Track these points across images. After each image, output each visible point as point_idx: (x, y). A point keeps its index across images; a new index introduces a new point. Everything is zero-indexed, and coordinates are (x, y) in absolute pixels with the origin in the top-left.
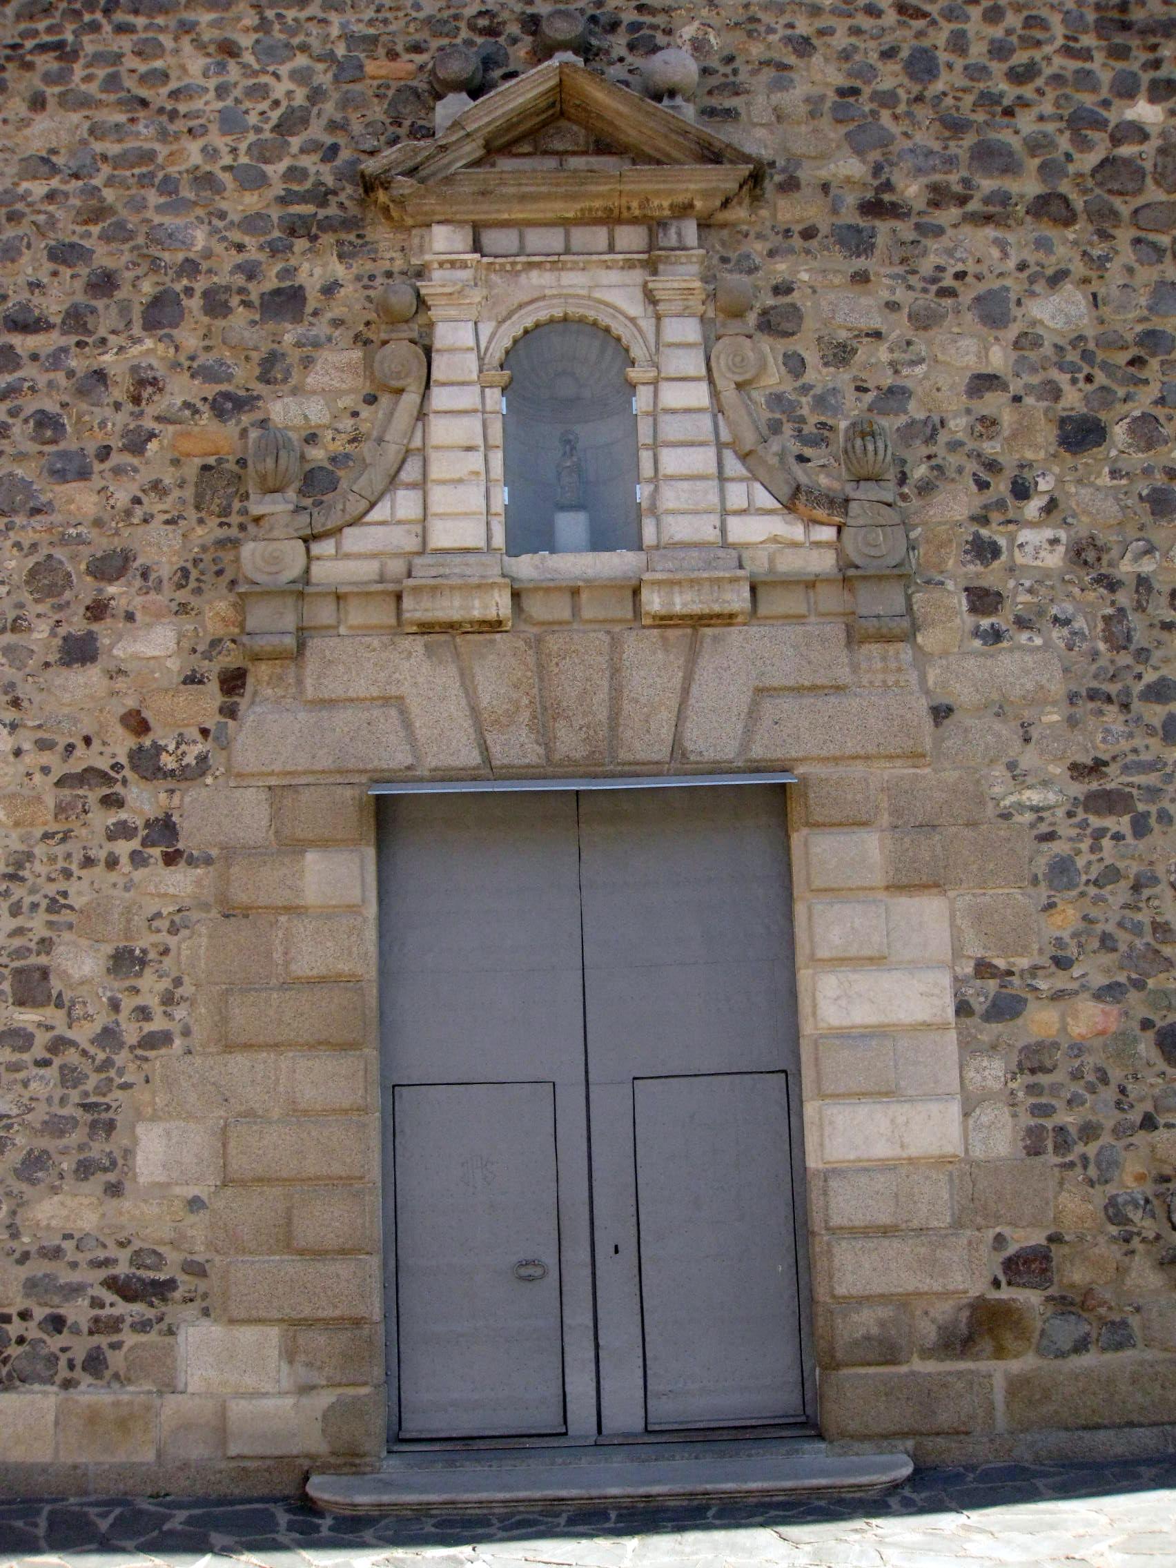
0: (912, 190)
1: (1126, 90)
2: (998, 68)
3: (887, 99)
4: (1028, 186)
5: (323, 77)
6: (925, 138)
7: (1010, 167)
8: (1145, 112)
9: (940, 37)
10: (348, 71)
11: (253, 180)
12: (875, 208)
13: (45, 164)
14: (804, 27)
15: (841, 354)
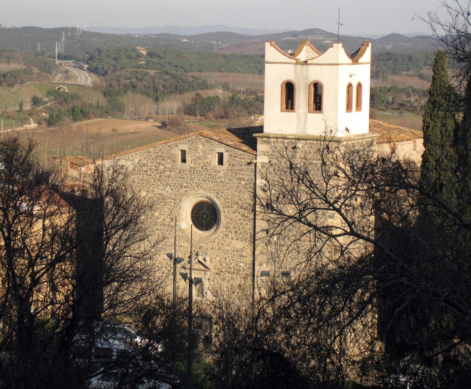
1: (241, 262)
2: (231, 259)
3: (223, 262)
5: (183, 254)
6: (225, 265)
8: (242, 265)
9: (227, 256)
10: (185, 254)
14: (217, 254)
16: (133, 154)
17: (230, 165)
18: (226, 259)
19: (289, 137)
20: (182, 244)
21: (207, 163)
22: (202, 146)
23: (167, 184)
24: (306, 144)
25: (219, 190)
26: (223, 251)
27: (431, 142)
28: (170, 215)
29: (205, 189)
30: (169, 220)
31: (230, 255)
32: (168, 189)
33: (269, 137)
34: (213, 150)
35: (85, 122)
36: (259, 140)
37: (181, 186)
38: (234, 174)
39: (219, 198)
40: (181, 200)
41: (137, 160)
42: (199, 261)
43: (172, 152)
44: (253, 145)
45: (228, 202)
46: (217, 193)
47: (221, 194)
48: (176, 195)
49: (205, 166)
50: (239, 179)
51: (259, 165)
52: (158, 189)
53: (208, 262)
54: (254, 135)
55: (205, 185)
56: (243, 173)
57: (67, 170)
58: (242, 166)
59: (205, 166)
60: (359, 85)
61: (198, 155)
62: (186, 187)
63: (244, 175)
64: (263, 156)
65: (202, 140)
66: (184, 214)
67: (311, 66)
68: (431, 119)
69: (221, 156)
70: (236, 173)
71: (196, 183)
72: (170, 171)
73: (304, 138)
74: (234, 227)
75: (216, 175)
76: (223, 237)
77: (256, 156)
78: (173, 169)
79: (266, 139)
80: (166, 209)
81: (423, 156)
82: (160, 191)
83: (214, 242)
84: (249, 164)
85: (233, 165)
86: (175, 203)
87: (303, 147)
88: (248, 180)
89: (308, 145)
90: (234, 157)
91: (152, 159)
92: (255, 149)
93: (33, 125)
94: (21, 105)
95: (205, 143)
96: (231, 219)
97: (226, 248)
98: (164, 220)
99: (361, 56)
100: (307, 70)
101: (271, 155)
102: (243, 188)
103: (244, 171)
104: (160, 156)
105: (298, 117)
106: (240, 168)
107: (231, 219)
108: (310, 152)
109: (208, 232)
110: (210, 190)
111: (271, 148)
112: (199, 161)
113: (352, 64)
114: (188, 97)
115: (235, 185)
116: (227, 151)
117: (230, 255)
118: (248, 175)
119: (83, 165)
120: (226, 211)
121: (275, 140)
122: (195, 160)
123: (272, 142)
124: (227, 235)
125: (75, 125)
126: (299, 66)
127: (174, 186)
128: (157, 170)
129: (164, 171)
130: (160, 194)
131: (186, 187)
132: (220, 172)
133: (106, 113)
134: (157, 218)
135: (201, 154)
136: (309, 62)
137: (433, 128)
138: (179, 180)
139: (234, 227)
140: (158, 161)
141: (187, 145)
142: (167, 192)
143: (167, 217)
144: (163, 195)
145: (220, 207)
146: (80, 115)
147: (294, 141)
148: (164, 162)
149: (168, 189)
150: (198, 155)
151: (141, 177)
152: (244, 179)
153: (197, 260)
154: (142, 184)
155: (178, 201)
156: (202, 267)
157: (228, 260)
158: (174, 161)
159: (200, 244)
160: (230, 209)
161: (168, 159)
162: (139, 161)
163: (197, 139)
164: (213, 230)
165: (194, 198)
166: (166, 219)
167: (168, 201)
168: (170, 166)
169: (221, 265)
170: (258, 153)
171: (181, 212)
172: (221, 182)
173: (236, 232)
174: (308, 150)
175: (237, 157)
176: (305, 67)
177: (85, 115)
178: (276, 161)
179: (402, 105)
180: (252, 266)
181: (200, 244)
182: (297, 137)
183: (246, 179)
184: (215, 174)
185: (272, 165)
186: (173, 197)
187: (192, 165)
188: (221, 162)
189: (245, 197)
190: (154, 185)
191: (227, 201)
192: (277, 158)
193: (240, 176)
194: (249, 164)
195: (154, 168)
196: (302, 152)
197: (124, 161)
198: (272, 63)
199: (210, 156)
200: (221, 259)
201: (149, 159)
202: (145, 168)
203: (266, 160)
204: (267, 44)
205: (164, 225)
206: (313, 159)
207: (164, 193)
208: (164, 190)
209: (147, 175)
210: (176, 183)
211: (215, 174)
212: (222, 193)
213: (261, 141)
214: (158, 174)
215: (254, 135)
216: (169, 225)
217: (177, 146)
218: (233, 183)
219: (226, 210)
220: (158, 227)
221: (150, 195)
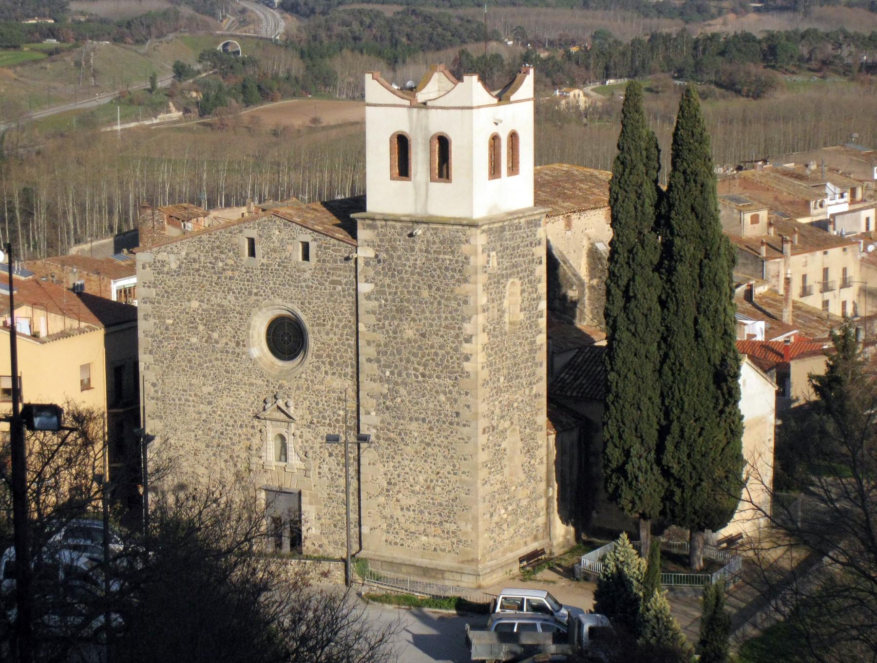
0: (315, 421)
1: (339, 409)
4: (327, 422)
6: (317, 414)
7: (325, 419)
10: (258, 397)
11: (249, 410)
12: (311, 423)
13: (228, 404)
15: (307, 442)
16: (178, 244)
17: (319, 261)
18: (317, 404)
19: (402, 218)
20: (253, 381)
21: (286, 258)
22: (277, 233)
23: (230, 289)
24: (428, 229)
25: (305, 299)
26: (314, 391)
27: (620, 223)
28: (234, 337)
29: (285, 298)
30: (234, 344)
31: (324, 398)
32: (231, 297)
33: (373, 219)
34: (294, 239)
36: (359, 223)
37: (250, 293)
38: (325, 275)
39: (305, 311)
40: (249, 314)
41: (183, 253)
42: (279, 408)
43: (235, 240)
44: (351, 229)
45: (319, 318)
46: (302, 303)
47: (307, 305)
48: (242, 306)
49: (283, 262)
50: (333, 282)
51: (361, 262)
52: (216, 297)
53: (292, 409)
54: (352, 216)
55: (283, 291)
56: (338, 272)
57: (163, 228)
58: (336, 262)
59: (283, 262)
60: (513, 137)
61: (272, 245)
62: (256, 294)
63: (340, 276)
64: (366, 247)
65: (278, 222)
66: (256, 335)
67: (434, 111)
68: (621, 188)
69: (306, 247)
70: (328, 273)
71: (271, 289)
72: (232, 270)
73: (424, 220)
74: (329, 356)
75: (300, 276)
76: (312, 371)
77: (356, 247)
78: (237, 266)
79: (370, 222)
80: (228, 328)
81: (611, 244)
82: (219, 301)
83: (300, 377)
84: (347, 259)
85: (324, 261)
86: (241, 319)
87: (424, 233)
88: (346, 284)
89: (431, 231)
90: (325, 248)
91: (207, 252)
92: (355, 236)
93: (176, 114)
94: (153, 80)
95: (282, 227)
96: (323, 343)
97: (317, 387)
98: (227, 344)
99: (516, 89)
100: (427, 117)
101: (379, 246)
102: (340, 295)
103: (340, 270)
104: (218, 247)
105: (416, 188)
106: (335, 265)
107: (323, 343)
108: (434, 243)
109: (288, 362)
110: (291, 298)
111: (378, 235)
112: (274, 255)
113: (498, 105)
115: (328, 291)
116: (315, 240)
117: (324, 398)
118: (346, 277)
119: (189, 220)
120: (316, 331)
121: (384, 223)
122: (268, 253)
123: (379, 226)
124: (318, 368)
125: (246, 113)
126: (415, 110)
127: (239, 293)
128: (213, 268)
129: (224, 270)
130: (219, 305)
131: (256, 294)
132: (305, 271)
134: (217, 342)
135: (277, 244)
136: (429, 104)
137: (623, 201)
138: (246, 283)
139: (329, 356)
140: (215, 255)
141: (256, 230)
142: (230, 302)
143: (230, 340)
144: (223, 306)
145: (307, 325)
147: (411, 224)
148: (223, 256)
149: (231, 297)
150: (272, 245)
151: (190, 278)
152: (341, 284)
153: (275, 406)
154: (193, 289)
155: (245, 316)
156: (282, 416)
157: (320, 406)
158: (238, 255)
159: (280, 382)
160: (321, 328)
161: (229, 251)
162: (187, 254)
163: (271, 221)
164: (298, 359)
165: (268, 310)
166: (230, 343)
167: (231, 315)
168: (233, 263)
169: (311, 413)
170: (359, 243)
171: (250, 332)
172: (307, 287)
173: (331, 364)
174: (431, 239)
175: (329, 248)
176: (423, 111)
177: (265, 94)
178: (385, 255)
179: (825, 63)
180: (355, 415)
181: (280, 382)
182: (414, 219)
183: (344, 282)
184: (298, 274)
185: (379, 261)
186: (238, 309)
187: (265, 261)
188: (306, 257)
189: (343, 310)
190: (209, 291)
191: (317, 315)
192: (387, 251)
193: (335, 278)
194: (347, 259)
195: (209, 265)
196: (423, 241)
197: (165, 254)
198: (375, 105)
199: (290, 247)
200: (311, 404)
201: (202, 251)
202: (196, 266)
203: (370, 253)
204: (368, 77)
205: (227, 352)
206: (439, 253)
207: (225, 303)
208: (225, 299)
209: (199, 275)
210: (241, 289)
211: (298, 274)
212: (309, 303)
213: (363, 225)
214: (215, 273)
215: (352, 216)
216: (233, 353)
217: (241, 231)
218: (325, 289)
219: (316, 329)
220: (219, 356)
221: (205, 306)
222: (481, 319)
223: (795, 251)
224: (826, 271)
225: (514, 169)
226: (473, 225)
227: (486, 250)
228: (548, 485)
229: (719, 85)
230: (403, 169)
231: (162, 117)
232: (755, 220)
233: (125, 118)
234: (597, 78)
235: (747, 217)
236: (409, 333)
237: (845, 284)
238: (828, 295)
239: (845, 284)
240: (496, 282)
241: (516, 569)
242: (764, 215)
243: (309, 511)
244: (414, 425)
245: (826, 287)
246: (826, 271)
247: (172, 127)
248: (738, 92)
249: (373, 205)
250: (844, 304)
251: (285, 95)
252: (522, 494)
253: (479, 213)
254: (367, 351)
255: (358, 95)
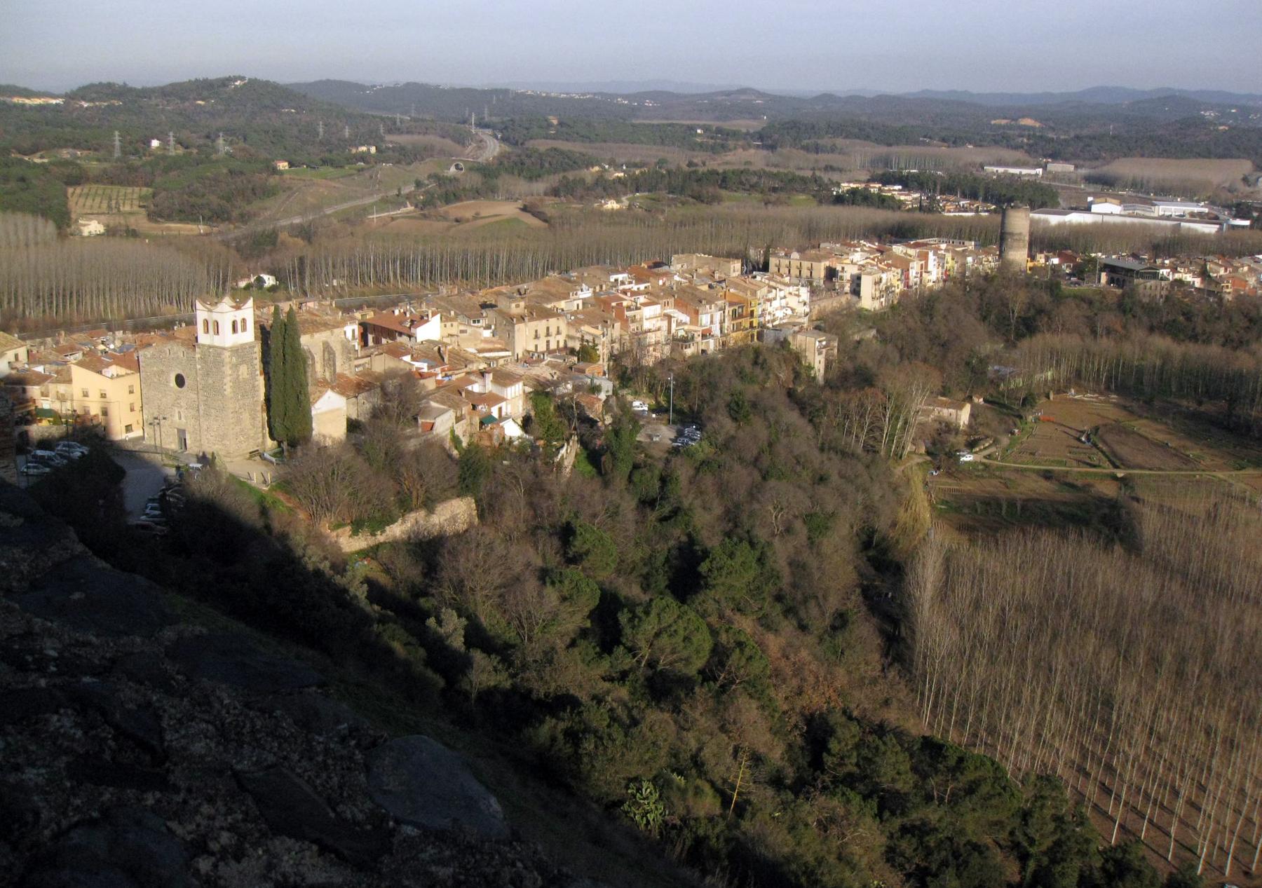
35: (459, 204)
60: (244, 320)
93: (410, 208)
94: (399, 190)
114: (554, 180)
125: (446, 208)
133: (477, 193)
146: (452, 197)
177: (457, 198)
179: (752, 186)
222: (229, 378)
223: (532, 319)
224: (548, 328)
225: (244, 329)
226: (224, 349)
227: (230, 357)
228: (263, 428)
229: (693, 197)
230: (207, 331)
231: (403, 210)
232: (518, 306)
233: (378, 212)
234: (632, 192)
235: (513, 305)
236: (210, 381)
237: (558, 333)
238: (549, 338)
239: (558, 333)
240: (235, 367)
241: (248, 456)
242: (522, 304)
243: (188, 437)
244: (213, 411)
245: (548, 335)
246: (548, 328)
247: (407, 216)
248: (702, 201)
249: (200, 341)
250: (558, 342)
251: (468, 199)
252: (251, 433)
253: (228, 344)
254: (200, 387)
255: (193, 306)
